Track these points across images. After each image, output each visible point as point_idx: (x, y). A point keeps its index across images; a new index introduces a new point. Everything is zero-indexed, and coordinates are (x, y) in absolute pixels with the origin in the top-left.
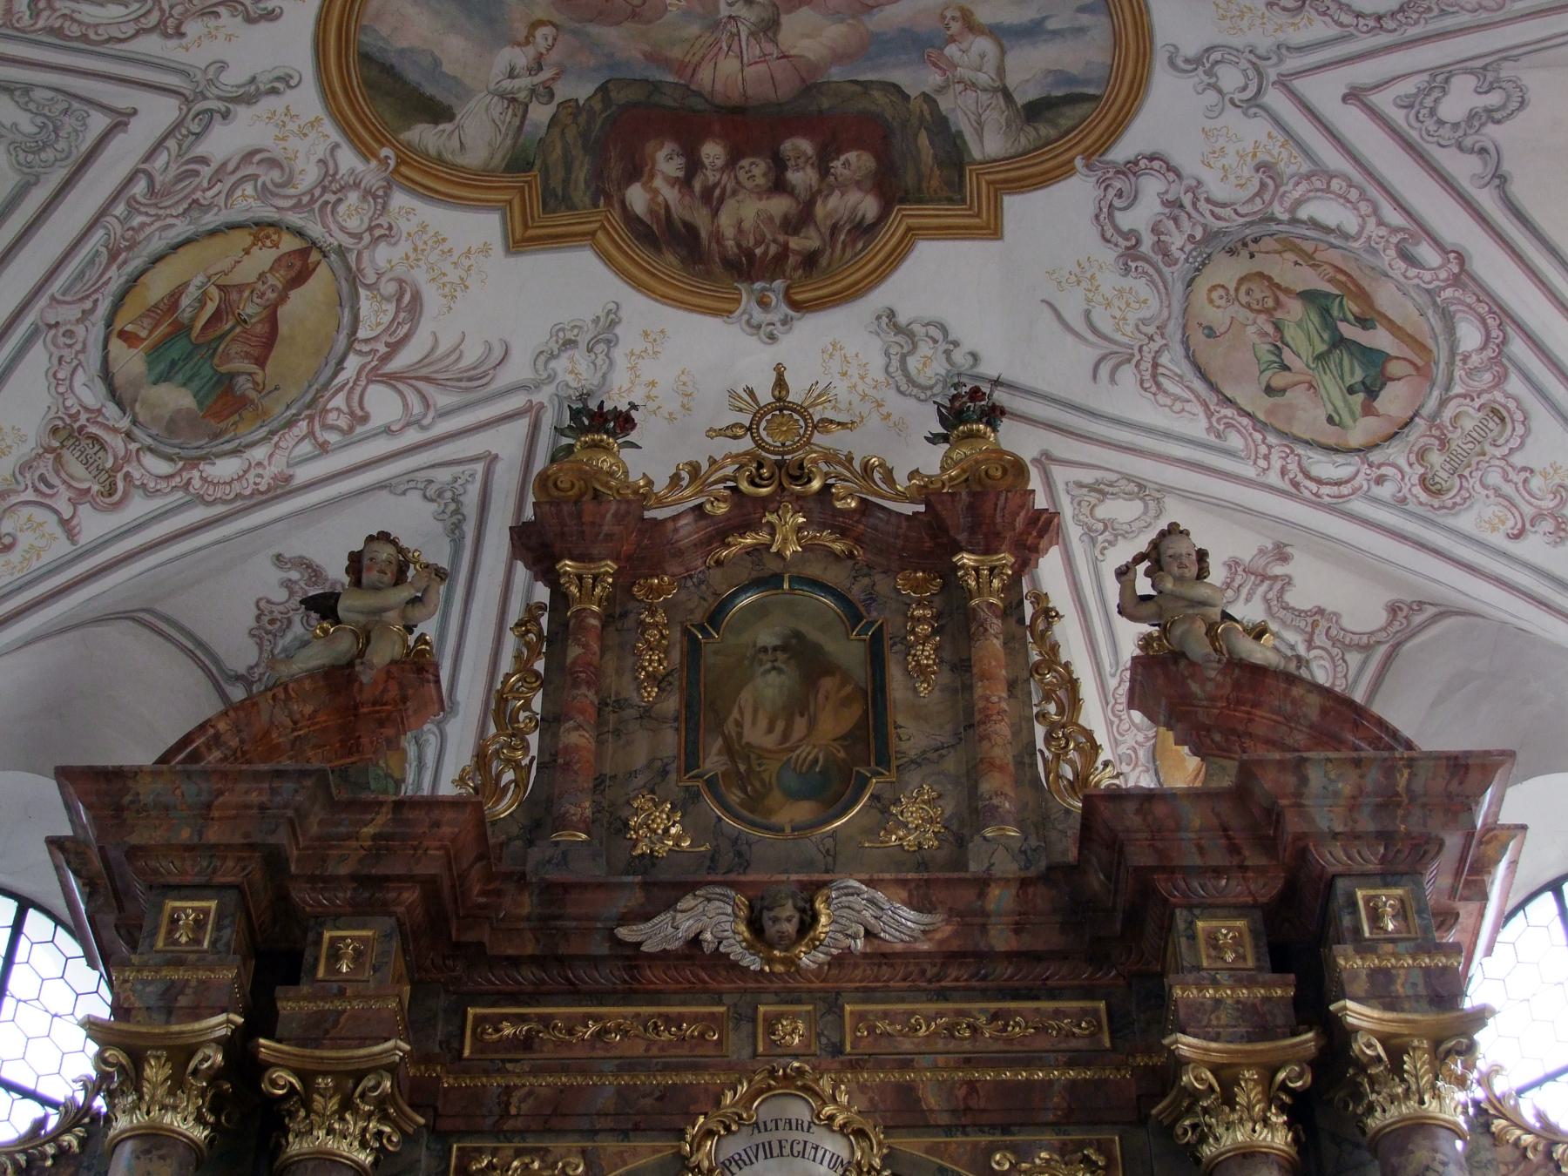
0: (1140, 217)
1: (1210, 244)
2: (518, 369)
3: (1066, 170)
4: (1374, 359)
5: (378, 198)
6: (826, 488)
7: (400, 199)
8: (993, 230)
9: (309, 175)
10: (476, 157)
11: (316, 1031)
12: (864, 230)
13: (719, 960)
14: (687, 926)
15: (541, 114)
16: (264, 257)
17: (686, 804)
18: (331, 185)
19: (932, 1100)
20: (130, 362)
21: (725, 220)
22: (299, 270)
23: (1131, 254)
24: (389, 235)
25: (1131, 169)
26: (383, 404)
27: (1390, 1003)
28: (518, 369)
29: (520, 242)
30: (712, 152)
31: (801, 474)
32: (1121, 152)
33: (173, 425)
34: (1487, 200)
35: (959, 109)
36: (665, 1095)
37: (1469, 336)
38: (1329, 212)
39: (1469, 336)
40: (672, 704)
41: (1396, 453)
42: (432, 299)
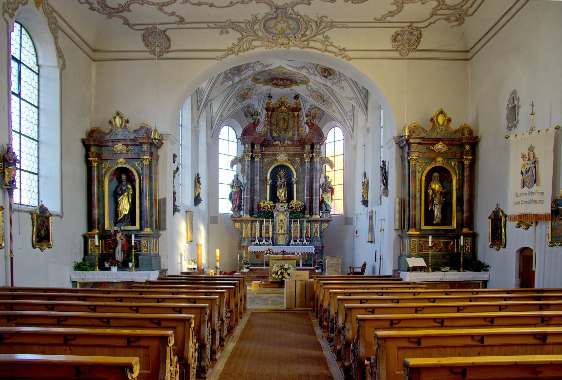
0: (309, 88)
1: (313, 91)
2: (264, 92)
3: (304, 84)
4: (324, 100)
5: (255, 85)
6: (286, 105)
7: (256, 84)
8: (299, 86)
9: (250, 85)
10: (262, 81)
11: (256, 153)
12: (289, 85)
13: (278, 145)
14: (277, 143)
15: (266, 79)
16: (247, 90)
17: (276, 132)
18: (252, 85)
19: (291, 154)
20: (238, 98)
21: (279, 83)
22: (249, 90)
23: (308, 90)
24: (256, 87)
25: (308, 85)
26: (255, 96)
27: (316, 153)
28: (264, 92)
29: (264, 85)
30: (279, 80)
31: (284, 104)
32: (308, 84)
33: (241, 101)
34: (332, 93)
35: (297, 80)
36: (275, 154)
37: (330, 100)
38: (321, 92)
39: (330, 100)
40: (275, 123)
41: (325, 105)
42: (258, 90)
